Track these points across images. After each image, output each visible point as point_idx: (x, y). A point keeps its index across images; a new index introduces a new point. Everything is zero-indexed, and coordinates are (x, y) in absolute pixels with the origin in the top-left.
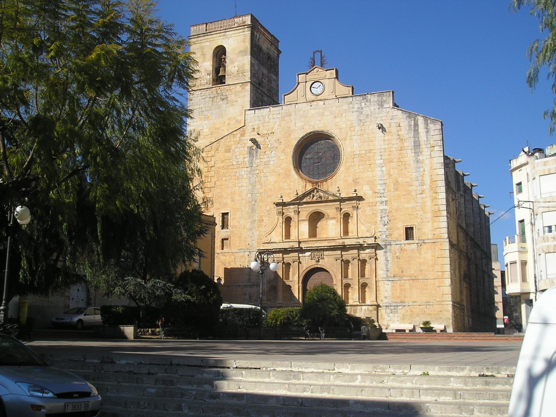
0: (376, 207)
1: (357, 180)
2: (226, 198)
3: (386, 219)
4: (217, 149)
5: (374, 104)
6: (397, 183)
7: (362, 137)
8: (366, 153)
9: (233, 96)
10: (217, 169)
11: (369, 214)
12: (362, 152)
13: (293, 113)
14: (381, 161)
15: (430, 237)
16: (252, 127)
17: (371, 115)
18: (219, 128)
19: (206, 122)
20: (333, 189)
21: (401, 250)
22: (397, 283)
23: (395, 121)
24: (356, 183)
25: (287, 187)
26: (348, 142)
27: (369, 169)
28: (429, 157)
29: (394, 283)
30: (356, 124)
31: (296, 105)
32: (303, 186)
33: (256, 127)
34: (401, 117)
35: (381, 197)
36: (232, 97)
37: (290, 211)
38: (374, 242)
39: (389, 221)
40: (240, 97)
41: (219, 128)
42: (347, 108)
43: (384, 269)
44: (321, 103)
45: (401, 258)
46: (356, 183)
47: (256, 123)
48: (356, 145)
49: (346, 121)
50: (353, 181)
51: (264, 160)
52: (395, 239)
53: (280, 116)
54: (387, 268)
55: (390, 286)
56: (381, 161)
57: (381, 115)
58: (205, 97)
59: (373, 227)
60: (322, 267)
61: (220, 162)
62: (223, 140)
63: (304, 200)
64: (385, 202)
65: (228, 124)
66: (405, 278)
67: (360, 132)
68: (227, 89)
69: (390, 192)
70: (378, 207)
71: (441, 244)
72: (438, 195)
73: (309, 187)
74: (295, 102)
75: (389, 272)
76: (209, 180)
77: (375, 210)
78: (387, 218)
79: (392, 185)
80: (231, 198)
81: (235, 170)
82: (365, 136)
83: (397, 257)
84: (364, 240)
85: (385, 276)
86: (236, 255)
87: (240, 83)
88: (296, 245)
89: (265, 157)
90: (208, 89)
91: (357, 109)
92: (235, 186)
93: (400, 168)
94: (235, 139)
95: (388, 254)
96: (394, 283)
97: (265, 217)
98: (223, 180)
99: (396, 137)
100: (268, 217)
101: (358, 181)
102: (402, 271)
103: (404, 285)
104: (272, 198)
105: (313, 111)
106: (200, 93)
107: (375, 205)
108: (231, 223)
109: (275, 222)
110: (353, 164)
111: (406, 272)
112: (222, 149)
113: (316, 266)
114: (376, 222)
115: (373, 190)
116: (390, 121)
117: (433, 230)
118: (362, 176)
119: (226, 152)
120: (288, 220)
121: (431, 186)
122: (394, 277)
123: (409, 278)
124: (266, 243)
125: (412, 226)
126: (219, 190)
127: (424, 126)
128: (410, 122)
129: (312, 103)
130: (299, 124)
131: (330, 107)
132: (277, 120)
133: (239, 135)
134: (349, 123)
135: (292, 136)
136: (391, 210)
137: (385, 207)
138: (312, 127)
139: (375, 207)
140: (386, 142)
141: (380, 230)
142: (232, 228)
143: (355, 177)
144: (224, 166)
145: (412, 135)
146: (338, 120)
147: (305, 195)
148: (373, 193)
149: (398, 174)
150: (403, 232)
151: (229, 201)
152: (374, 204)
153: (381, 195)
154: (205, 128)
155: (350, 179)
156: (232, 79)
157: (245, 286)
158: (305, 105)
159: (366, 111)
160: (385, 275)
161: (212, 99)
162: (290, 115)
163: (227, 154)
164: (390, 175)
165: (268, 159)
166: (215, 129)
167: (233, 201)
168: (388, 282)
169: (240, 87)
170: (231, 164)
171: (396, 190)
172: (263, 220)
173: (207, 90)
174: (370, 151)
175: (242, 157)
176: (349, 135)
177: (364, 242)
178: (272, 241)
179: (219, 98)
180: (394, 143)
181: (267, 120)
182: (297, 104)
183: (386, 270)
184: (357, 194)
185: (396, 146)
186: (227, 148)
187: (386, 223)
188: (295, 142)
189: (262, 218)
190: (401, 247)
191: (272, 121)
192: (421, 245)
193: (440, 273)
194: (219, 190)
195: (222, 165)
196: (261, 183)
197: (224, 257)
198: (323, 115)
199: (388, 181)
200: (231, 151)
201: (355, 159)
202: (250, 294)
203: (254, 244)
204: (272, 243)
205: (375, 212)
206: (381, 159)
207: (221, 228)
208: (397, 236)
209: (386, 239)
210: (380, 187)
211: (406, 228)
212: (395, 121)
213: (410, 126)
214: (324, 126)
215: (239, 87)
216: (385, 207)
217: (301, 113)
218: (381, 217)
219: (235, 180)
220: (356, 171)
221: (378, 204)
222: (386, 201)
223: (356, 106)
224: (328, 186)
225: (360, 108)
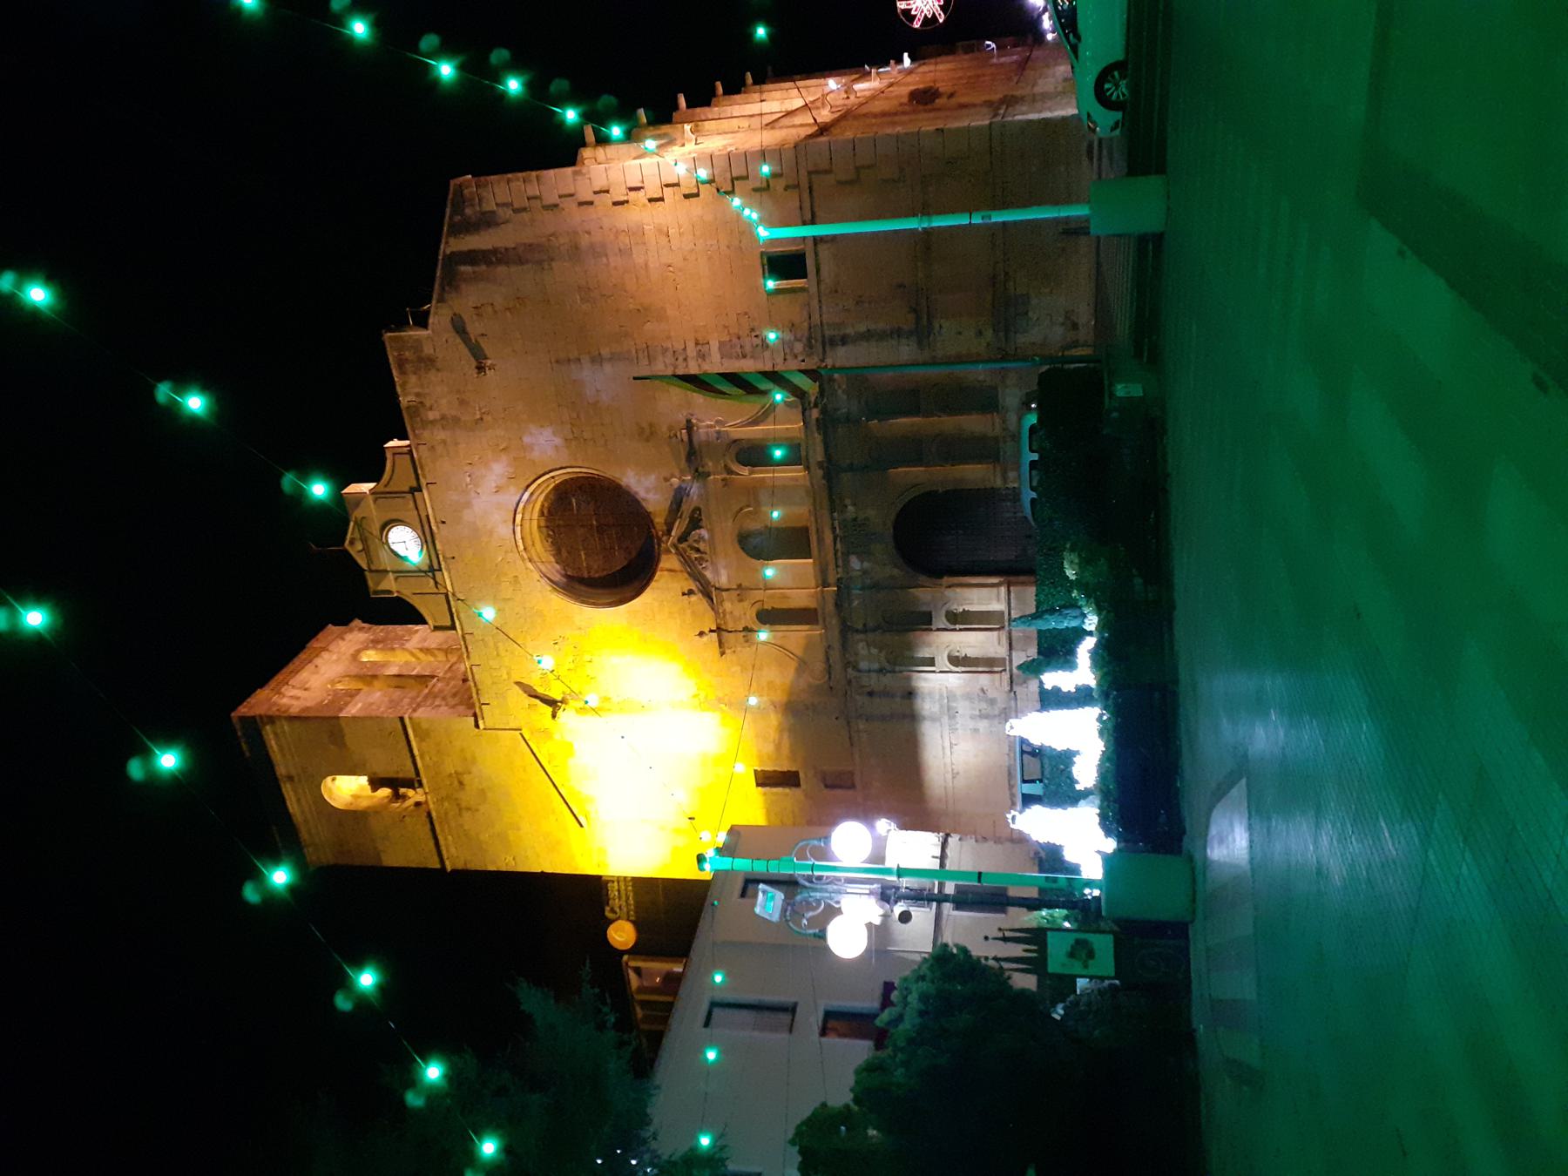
35: (685, 359)
39: (754, 334)
50: (647, 440)
55: (946, 324)
64: (699, 347)
75: (901, 325)
95: (849, 331)
122: (915, 311)
137: (714, 346)
153: (681, 359)
183: (896, 336)
187: (758, 341)
201: (586, 435)
202: (972, 717)
213: (476, 278)
218: (744, 356)
225: (445, 423)
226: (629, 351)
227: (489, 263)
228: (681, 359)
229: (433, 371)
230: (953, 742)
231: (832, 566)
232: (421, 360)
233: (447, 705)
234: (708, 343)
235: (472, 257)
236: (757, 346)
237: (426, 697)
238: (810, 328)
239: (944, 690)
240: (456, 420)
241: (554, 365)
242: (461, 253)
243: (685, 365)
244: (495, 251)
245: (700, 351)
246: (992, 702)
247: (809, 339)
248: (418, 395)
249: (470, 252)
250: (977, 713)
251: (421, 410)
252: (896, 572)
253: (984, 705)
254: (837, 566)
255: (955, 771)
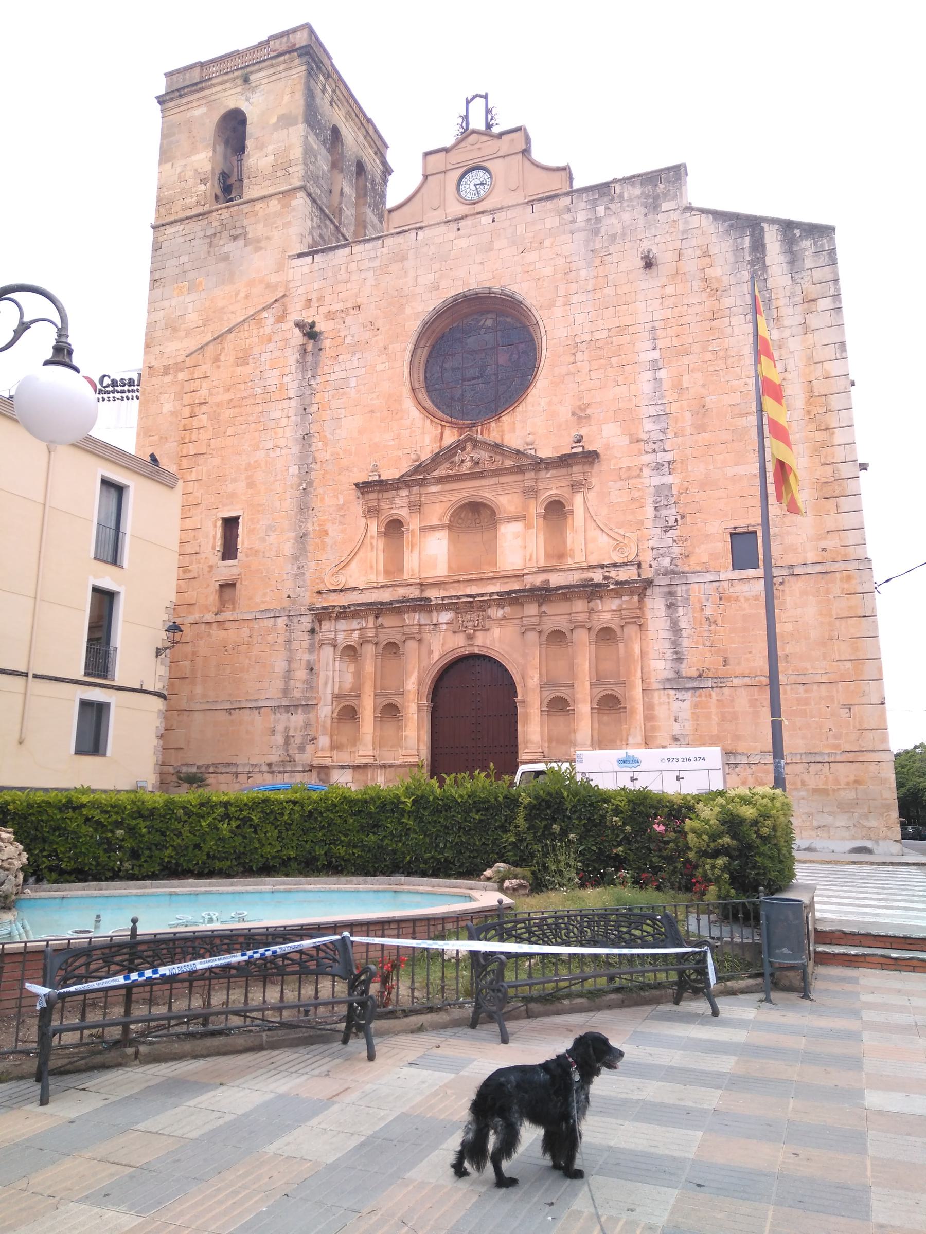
0: (642, 480)
1: (585, 410)
2: (235, 480)
3: (671, 513)
4: (217, 360)
5: (633, 206)
6: (701, 410)
7: (598, 295)
8: (609, 337)
9: (260, 226)
10: (215, 408)
11: (620, 500)
12: (597, 335)
13: (411, 254)
14: (656, 355)
15: (811, 557)
16: (304, 298)
17: (624, 234)
18: (223, 308)
19: (193, 296)
20: (514, 440)
21: (721, 599)
22: (710, 695)
23: (694, 242)
24: (580, 418)
25: (392, 443)
26: (558, 312)
27: (620, 379)
28: (800, 329)
29: (700, 696)
30: (582, 263)
31: (420, 233)
32: (436, 436)
33: (314, 296)
34: (712, 229)
35: (654, 451)
36: (256, 230)
37: (399, 505)
38: (636, 578)
39: (679, 517)
40: (276, 227)
41: (223, 308)
42: (557, 224)
43: (666, 656)
44: (486, 220)
45: (719, 622)
46: (580, 418)
47: (316, 286)
48: (580, 318)
49: (553, 258)
50: (574, 414)
51: (333, 377)
52: (699, 569)
53: (376, 263)
54: (676, 653)
55: (687, 705)
56: (656, 355)
57: (653, 232)
58: (192, 237)
59: (634, 536)
60: (484, 652)
61: (221, 390)
62: (231, 336)
63: (437, 473)
64: (666, 465)
65: (247, 297)
66: (736, 682)
67: (592, 282)
68: (244, 212)
69: (683, 436)
70: (647, 482)
71: (849, 578)
72: (833, 434)
73: (450, 437)
74: (418, 225)
75: (685, 661)
76: (194, 438)
77: (639, 489)
78: (673, 511)
79: (688, 415)
80: (247, 478)
81: (259, 409)
82: (607, 291)
83: (707, 619)
84: (607, 574)
85: (671, 675)
86: (255, 625)
87: (280, 193)
88: (414, 593)
89: (336, 368)
90: (200, 218)
91: (583, 224)
92: (256, 448)
93: (711, 369)
94: (262, 329)
95: (681, 612)
96: (700, 696)
97: (333, 523)
98: (228, 434)
99: (697, 285)
100: (340, 523)
101: (589, 412)
102: (725, 661)
103: (732, 701)
104: (351, 474)
105: (463, 243)
106: (180, 229)
107: (639, 476)
108: (246, 543)
109: (359, 536)
110: (572, 368)
111: (739, 664)
112: (228, 356)
113: (467, 651)
114: (642, 522)
115: (631, 435)
116: (678, 244)
117: (820, 538)
118: (599, 400)
119: (238, 365)
120: (395, 527)
121: (809, 412)
122: (700, 676)
123: (747, 681)
124: (335, 591)
125: (751, 529)
126: (216, 461)
127: (781, 247)
128: (739, 240)
129: (462, 224)
130: (427, 279)
131: (510, 225)
132: (370, 274)
133: (271, 320)
134: (561, 261)
135: (408, 311)
136: (686, 485)
137: (669, 479)
138: (461, 283)
139: (638, 480)
140: (669, 302)
141: (652, 543)
142: (247, 556)
143: (579, 403)
144: (231, 400)
145: (746, 275)
146: (532, 257)
147: (437, 459)
148: (631, 443)
149: (704, 386)
150: (724, 546)
151: (241, 486)
152: (635, 473)
153: (654, 446)
154: (190, 310)
155: (565, 412)
156: (260, 186)
157: (275, 709)
158: (443, 228)
159: (612, 224)
160: (672, 671)
161: (208, 240)
162: (403, 258)
163: (239, 370)
164: (679, 389)
165: (343, 375)
166: (214, 312)
167: (251, 485)
168: (680, 695)
169: (279, 202)
170: (249, 392)
171: (701, 428)
172: (326, 533)
173: (197, 219)
174: (622, 329)
175: (276, 373)
176: (561, 293)
177: (606, 578)
178: (352, 584)
179: (225, 234)
180: (692, 301)
181: (343, 275)
182: (421, 228)
183: (675, 656)
184: (583, 447)
185: (698, 309)
186: (241, 355)
187: (671, 522)
188: (414, 326)
189: (325, 528)
190: (721, 589)
191: (355, 277)
192: (781, 583)
193: (849, 665)
194: (216, 461)
195: (227, 396)
196: (325, 436)
197: (222, 634)
198: (491, 250)
199: (674, 407)
200: (251, 361)
201: (579, 356)
202: (287, 729)
203: (302, 595)
204: (349, 589)
205: (637, 494)
206: (655, 348)
207: (217, 558)
208: (705, 559)
209: (672, 567)
210: (652, 424)
211: (731, 534)
212: (694, 242)
213: (738, 250)
214: (494, 278)
215: (276, 202)
216: (669, 479)
217: (433, 249)
218: (656, 509)
219: (257, 433)
220: (582, 388)
221: (647, 472)
222: (669, 462)
223: (581, 217)
224: (503, 431)
225: (593, 221)
226: (663, 397)
227: (752, 263)
228: (654, 446)
229: (644, 210)
230: (262, 710)
231: (443, 594)
232: (656, 198)
233: (313, 227)
234: (670, 473)
235: (758, 246)
236: (667, 521)
237: (322, 210)
238: (683, 573)
239: (315, 702)
240: (596, 232)
241: (649, 325)
242: (762, 237)
243: (650, 451)
244: (765, 268)
245: (663, 465)
246: (302, 749)
247: (673, 572)
248: (621, 196)
249: (764, 246)
250: (291, 734)
251: (606, 199)
252: (436, 656)
253: (298, 740)
254: (443, 598)
255: (233, 711)
